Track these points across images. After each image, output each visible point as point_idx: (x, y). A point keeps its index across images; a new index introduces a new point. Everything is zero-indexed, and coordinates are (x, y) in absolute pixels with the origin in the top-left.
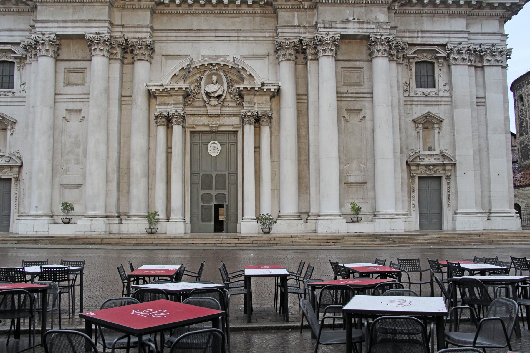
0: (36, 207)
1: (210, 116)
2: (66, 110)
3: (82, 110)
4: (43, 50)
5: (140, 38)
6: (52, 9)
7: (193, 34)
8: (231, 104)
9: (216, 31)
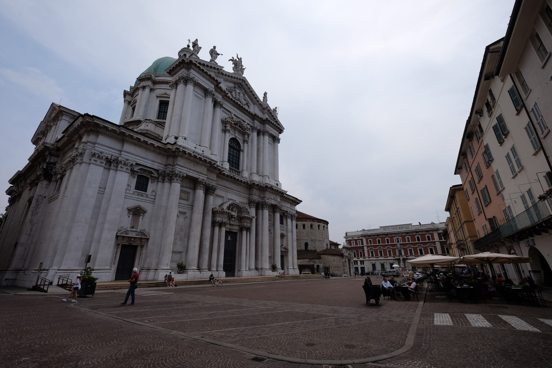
0: (167, 264)
1: (230, 224)
2: (179, 211)
3: (186, 213)
4: (175, 179)
5: (213, 186)
6: (184, 161)
7: (226, 189)
8: (237, 221)
9: (234, 190)
